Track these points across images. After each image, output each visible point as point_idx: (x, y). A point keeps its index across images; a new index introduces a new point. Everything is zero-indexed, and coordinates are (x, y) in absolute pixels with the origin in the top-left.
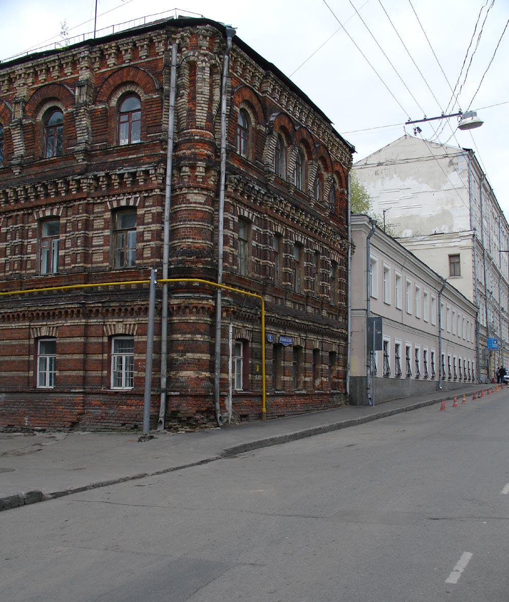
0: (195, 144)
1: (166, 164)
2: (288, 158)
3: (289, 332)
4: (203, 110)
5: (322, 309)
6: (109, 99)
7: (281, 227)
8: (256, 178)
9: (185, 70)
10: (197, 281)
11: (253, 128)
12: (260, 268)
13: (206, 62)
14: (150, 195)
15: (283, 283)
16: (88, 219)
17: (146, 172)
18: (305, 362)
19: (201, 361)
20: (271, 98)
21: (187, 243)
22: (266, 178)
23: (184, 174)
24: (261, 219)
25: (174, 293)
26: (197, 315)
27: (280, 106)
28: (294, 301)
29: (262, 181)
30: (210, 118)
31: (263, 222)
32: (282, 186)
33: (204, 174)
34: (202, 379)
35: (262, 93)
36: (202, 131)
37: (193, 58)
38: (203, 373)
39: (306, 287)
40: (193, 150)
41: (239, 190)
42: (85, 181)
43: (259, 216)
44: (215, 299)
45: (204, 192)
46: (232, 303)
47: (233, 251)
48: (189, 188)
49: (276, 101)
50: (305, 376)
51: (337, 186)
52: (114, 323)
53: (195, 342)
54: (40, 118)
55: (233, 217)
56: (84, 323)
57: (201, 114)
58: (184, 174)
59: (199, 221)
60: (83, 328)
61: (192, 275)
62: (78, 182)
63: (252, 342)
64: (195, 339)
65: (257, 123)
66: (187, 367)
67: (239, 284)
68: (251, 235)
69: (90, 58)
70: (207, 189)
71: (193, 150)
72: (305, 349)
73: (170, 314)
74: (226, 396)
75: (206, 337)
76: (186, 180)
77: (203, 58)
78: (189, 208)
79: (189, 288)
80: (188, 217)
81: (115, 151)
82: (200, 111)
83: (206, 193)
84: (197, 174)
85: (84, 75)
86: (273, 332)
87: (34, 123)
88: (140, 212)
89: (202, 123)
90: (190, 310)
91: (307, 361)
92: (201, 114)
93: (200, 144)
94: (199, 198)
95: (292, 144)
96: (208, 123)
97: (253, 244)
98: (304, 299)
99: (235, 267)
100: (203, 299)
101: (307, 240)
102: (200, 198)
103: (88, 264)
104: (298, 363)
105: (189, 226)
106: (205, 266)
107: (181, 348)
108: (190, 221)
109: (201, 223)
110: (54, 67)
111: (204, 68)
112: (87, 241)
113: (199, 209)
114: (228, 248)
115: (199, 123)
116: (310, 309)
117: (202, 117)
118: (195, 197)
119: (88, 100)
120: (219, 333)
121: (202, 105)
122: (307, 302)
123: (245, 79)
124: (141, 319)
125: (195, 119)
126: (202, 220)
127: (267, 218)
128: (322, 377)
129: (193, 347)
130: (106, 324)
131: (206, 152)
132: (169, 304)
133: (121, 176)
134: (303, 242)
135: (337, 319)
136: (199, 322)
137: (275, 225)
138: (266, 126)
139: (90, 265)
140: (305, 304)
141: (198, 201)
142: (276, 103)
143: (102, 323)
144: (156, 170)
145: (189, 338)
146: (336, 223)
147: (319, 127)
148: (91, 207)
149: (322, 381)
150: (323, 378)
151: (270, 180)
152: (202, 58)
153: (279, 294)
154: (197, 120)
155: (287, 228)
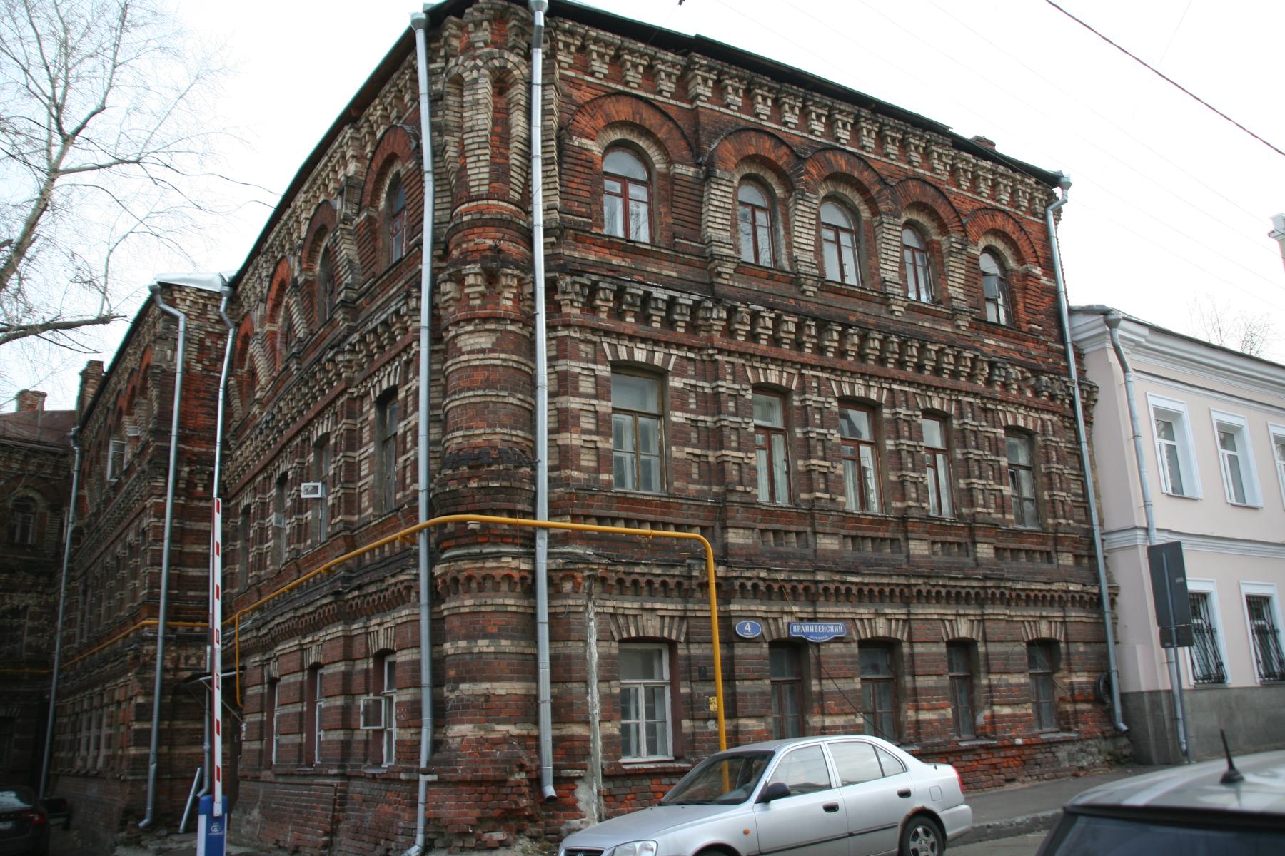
0: (467, 232)
1: (420, 290)
2: (792, 220)
3: (822, 610)
4: (479, 161)
5: (974, 543)
6: (375, 197)
7: (781, 372)
8: (674, 274)
9: (450, 98)
10: (474, 520)
11: (660, 174)
12: (710, 471)
13: (479, 68)
14: (411, 356)
15: (804, 496)
16: (353, 427)
17: (397, 312)
18: (914, 675)
19: (493, 699)
20: (722, 110)
21: (456, 441)
22: (711, 271)
23: (446, 298)
24: (704, 361)
25: (443, 552)
26: (482, 594)
27: (757, 120)
28: (854, 533)
29: (698, 279)
30: (500, 172)
31: (709, 367)
32: (772, 283)
33: (482, 289)
34: (495, 743)
35: (692, 101)
36: (480, 202)
37: (456, 69)
38: (498, 728)
39: (898, 496)
40: (464, 246)
41: (599, 306)
42: (340, 358)
43: (691, 355)
44: (532, 556)
45: (488, 326)
46: (593, 558)
47: (595, 442)
48: (456, 323)
49: (734, 111)
50: (917, 709)
51: (1012, 264)
52: (376, 628)
53: (475, 656)
54: (317, 269)
55: (592, 366)
56: (340, 634)
57: (476, 171)
58: (446, 298)
59: (479, 388)
60: (341, 641)
61: (461, 508)
62: (332, 360)
63: (688, 642)
64: (476, 650)
65: (670, 162)
66: (462, 714)
67: (623, 514)
68: (669, 400)
69: (357, 139)
70: (498, 319)
71: (464, 246)
72: (911, 642)
73: (436, 598)
74: (580, 778)
75: (504, 642)
76: (451, 309)
77: (472, 63)
78: (459, 366)
79: (463, 536)
80: (458, 385)
81: (378, 290)
82: (473, 165)
83: (493, 326)
84: (467, 291)
85: (352, 168)
86: (758, 614)
87: (311, 279)
88: (401, 395)
89: (482, 188)
90: (479, 584)
91: (918, 670)
92: (476, 171)
93: (476, 230)
94: (477, 340)
95: (794, 189)
96: (494, 185)
97: (674, 419)
98: (892, 524)
99: (604, 477)
100: (483, 557)
101: (890, 390)
102: (483, 340)
103: (354, 515)
104: (897, 676)
105: (458, 403)
106: (484, 484)
107: (452, 673)
108: (461, 391)
109: (480, 392)
110: (328, 176)
111: (475, 81)
112: (351, 470)
113: (477, 363)
114: (575, 436)
115: (476, 189)
116: (919, 548)
117: (481, 176)
118: (472, 341)
119: (349, 212)
120: (544, 632)
121: (477, 152)
122: (906, 531)
123: (627, 84)
124: (396, 615)
125: (467, 183)
126: (488, 385)
127: (717, 357)
128: (992, 704)
129: (477, 669)
130: (371, 629)
131: (490, 242)
132: (432, 577)
133: (374, 330)
134: (873, 396)
135: (1050, 560)
136: (483, 609)
137: (753, 367)
138: (698, 165)
139: (356, 517)
140: (900, 536)
141: (478, 347)
142: (738, 114)
143: (363, 631)
144: (407, 303)
145: (464, 648)
146: (1003, 341)
147: (904, 145)
148: (358, 404)
149: (993, 716)
150: (996, 708)
151: (719, 274)
152: (470, 64)
153: (791, 523)
154: (472, 184)
155: (803, 371)
